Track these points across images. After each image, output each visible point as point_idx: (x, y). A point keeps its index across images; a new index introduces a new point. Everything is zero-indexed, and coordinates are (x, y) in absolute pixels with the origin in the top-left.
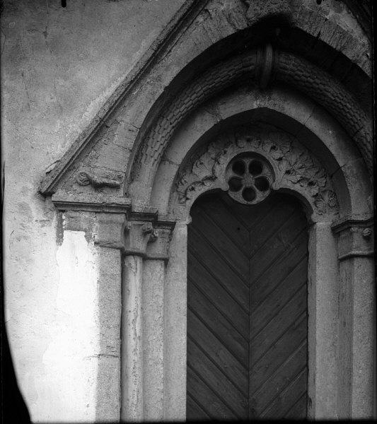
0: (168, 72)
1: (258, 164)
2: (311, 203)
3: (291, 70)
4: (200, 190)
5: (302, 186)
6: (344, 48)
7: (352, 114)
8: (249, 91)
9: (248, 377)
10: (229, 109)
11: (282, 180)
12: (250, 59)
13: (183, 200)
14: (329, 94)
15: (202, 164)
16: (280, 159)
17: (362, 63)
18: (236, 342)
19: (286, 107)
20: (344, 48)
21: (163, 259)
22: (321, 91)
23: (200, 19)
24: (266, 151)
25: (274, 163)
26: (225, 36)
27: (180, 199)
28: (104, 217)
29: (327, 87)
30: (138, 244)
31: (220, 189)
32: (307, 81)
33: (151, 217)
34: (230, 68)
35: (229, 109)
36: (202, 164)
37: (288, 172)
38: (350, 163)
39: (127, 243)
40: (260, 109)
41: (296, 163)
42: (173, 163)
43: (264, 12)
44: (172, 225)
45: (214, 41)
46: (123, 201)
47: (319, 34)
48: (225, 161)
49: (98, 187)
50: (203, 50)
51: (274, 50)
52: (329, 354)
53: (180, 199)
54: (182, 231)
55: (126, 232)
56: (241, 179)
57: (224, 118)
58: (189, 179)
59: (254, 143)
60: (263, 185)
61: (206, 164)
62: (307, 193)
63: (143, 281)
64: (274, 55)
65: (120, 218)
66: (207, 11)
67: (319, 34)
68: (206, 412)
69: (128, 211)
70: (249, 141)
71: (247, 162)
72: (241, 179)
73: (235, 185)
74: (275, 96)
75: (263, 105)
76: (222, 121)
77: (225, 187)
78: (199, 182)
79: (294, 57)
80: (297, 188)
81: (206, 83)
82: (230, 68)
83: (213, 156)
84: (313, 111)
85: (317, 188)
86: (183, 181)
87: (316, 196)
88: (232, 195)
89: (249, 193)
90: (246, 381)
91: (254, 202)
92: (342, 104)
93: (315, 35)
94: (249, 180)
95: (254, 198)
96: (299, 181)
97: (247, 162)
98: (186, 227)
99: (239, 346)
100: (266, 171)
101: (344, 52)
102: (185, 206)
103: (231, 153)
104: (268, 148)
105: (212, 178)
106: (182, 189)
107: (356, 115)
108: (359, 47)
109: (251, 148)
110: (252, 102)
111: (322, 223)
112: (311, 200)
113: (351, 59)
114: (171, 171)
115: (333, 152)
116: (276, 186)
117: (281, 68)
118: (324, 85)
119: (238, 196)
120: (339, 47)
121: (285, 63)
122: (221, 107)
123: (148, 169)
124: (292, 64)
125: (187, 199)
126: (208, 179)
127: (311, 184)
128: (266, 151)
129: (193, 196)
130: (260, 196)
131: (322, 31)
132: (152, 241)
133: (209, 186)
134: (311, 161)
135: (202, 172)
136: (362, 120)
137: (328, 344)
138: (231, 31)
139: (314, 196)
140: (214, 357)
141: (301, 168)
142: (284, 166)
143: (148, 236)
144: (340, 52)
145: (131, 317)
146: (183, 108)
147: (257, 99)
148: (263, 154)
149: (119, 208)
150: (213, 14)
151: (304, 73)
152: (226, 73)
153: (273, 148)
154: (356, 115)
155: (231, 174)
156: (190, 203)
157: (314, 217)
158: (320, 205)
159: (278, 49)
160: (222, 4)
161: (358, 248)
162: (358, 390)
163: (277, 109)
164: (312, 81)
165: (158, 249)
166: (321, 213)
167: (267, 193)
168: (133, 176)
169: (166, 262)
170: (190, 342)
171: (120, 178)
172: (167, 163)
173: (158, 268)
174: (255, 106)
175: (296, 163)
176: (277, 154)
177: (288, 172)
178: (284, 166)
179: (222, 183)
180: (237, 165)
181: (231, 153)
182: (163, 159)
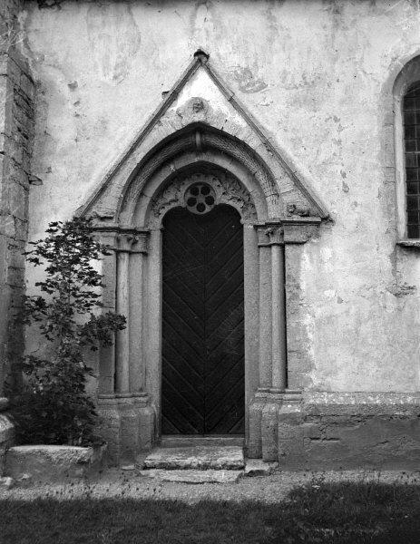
0: (140, 155)
1: (207, 189)
4: (168, 208)
10: (181, 163)
21: (143, 253)
23: (156, 126)
28: (106, 234)
30: (126, 247)
33: (134, 232)
35: (181, 163)
37: (224, 194)
39: (119, 246)
43: (190, 121)
44: (148, 234)
45: (164, 137)
46: (117, 225)
48: (183, 189)
49: (102, 219)
55: (118, 240)
58: (161, 202)
60: (210, 201)
62: (238, 206)
63: (129, 265)
65: (114, 234)
69: (119, 230)
70: (198, 176)
71: (200, 188)
73: (191, 202)
80: (231, 203)
88: (188, 207)
89: (201, 207)
94: (201, 199)
95: (204, 209)
97: (200, 188)
106: (156, 208)
109: (202, 180)
110: (194, 159)
112: (239, 210)
114: (146, 201)
116: (217, 203)
119: (193, 210)
123: (131, 204)
127: (239, 200)
129: (163, 212)
130: (208, 209)
132: (135, 243)
133: (173, 205)
135: (169, 197)
138: (173, 131)
142: (222, 190)
143: (132, 241)
145: (121, 286)
149: (113, 229)
152: (160, 158)
155: (189, 195)
157: (242, 221)
165: (139, 247)
166: (246, 218)
168: (122, 207)
169: (145, 254)
171: (113, 213)
173: (139, 258)
177: (224, 194)
178: (222, 190)
179: (182, 203)
180: (193, 190)
181: (188, 184)
182: (142, 194)
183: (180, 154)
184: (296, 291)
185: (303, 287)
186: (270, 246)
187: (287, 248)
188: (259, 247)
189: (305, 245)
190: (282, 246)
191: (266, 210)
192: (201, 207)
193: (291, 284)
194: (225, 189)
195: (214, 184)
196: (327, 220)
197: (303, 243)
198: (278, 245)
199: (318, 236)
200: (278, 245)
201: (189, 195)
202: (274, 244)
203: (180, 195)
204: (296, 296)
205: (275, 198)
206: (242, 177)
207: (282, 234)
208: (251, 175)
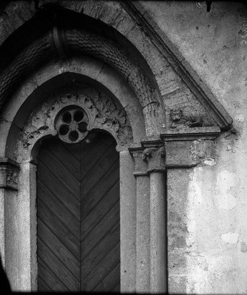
1: (80, 114)
2: (116, 138)
3: (75, 41)
4: (37, 137)
5: (108, 125)
6: (101, 16)
7: (121, 65)
8: (55, 63)
9: (80, 267)
10: (44, 77)
11: (94, 122)
12: (46, 40)
13: (26, 145)
14: (103, 54)
15: (38, 118)
16: (91, 108)
17: (116, 25)
18: (72, 243)
19: (82, 68)
20: (101, 16)
22: (98, 52)
24: (85, 105)
25: (87, 110)
26: (17, 27)
27: (24, 145)
29: (101, 49)
31: (50, 135)
32: (88, 47)
34: (33, 49)
35: (44, 77)
36: (38, 118)
37: (97, 116)
38: (132, 104)
40: (64, 74)
41: (103, 109)
42: (7, 121)
45: (10, 33)
47: (83, 10)
48: (53, 114)
50: (3, 41)
51: (59, 30)
52: (131, 251)
53: (24, 145)
54: (26, 167)
56: (68, 126)
57: (39, 85)
59: (73, 98)
60: (83, 127)
61: (41, 119)
62: (112, 130)
64: (59, 34)
66: (5, 13)
67: (83, 10)
68: (68, 289)
70: (69, 97)
71: (72, 112)
72: (68, 126)
73: (63, 130)
74: (74, 62)
75: (65, 70)
76: (38, 87)
77: (54, 133)
78: (35, 132)
79: (76, 31)
80: (105, 127)
81: (18, 63)
82: (33, 49)
83: (46, 112)
84: (103, 68)
85: (119, 125)
86: (25, 132)
87: (118, 132)
88: (62, 138)
90: (78, 269)
91: (77, 141)
92: (113, 59)
93: (80, 11)
94: (73, 126)
96: (105, 122)
97: (72, 112)
98: (29, 164)
99: (73, 245)
100: (85, 117)
101: (101, 19)
102: (28, 149)
103: (58, 108)
104: (83, 101)
105: (45, 128)
107: (123, 65)
108: (113, 12)
111: (123, 152)
112: (114, 134)
113: (107, 23)
115: (118, 97)
116: (89, 128)
117: (68, 41)
118: (99, 47)
119: (66, 139)
120: (97, 16)
121: (70, 37)
122: (38, 77)
124: (75, 37)
125: (29, 144)
126: (41, 128)
127: (114, 123)
128: (85, 105)
129: (33, 142)
130: (81, 136)
131: (84, 8)
133: (43, 133)
134: (114, 106)
136: (128, 68)
137: (130, 244)
138: (21, 23)
139: (117, 132)
140: (57, 253)
141: (107, 112)
144: (99, 20)
146: (3, 83)
147: (61, 67)
148: (80, 105)
150: (9, 14)
151: (84, 41)
153: (86, 100)
154: (123, 65)
155: (61, 123)
156: (31, 147)
157: (118, 148)
158: (122, 138)
159: (62, 28)
160: (15, 6)
161: (138, 169)
162: (141, 280)
163: (76, 71)
164: (90, 46)
167: (86, 133)
170: (40, 241)
172: (4, 122)
174: (60, 72)
175: (103, 109)
176: (90, 104)
177: (97, 116)
178: (94, 112)
179: (52, 131)
180: (65, 115)
181: (58, 108)
183: (42, 63)
184: (181, 234)
185: (191, 227)
186: (148, 175)
187: (171, 174)
188: (136, 176)
189: (195, 169)
190: (163, 174)
191: (143, 126)
192: (74, 135)
193: (175, 224)
194: (98, 110)
195: (84, 104)
196: (228, 129)
197: (191, 167)
198: (158, 171)
199: (214, 155)
200: (158, 171)
201: (61, 123)
202: (153, 171)
203: (50, 122)
204: (181, 242)
205: (153, 107)
206: (114, 87)
207: (164, 157)
208: (125, 82)
